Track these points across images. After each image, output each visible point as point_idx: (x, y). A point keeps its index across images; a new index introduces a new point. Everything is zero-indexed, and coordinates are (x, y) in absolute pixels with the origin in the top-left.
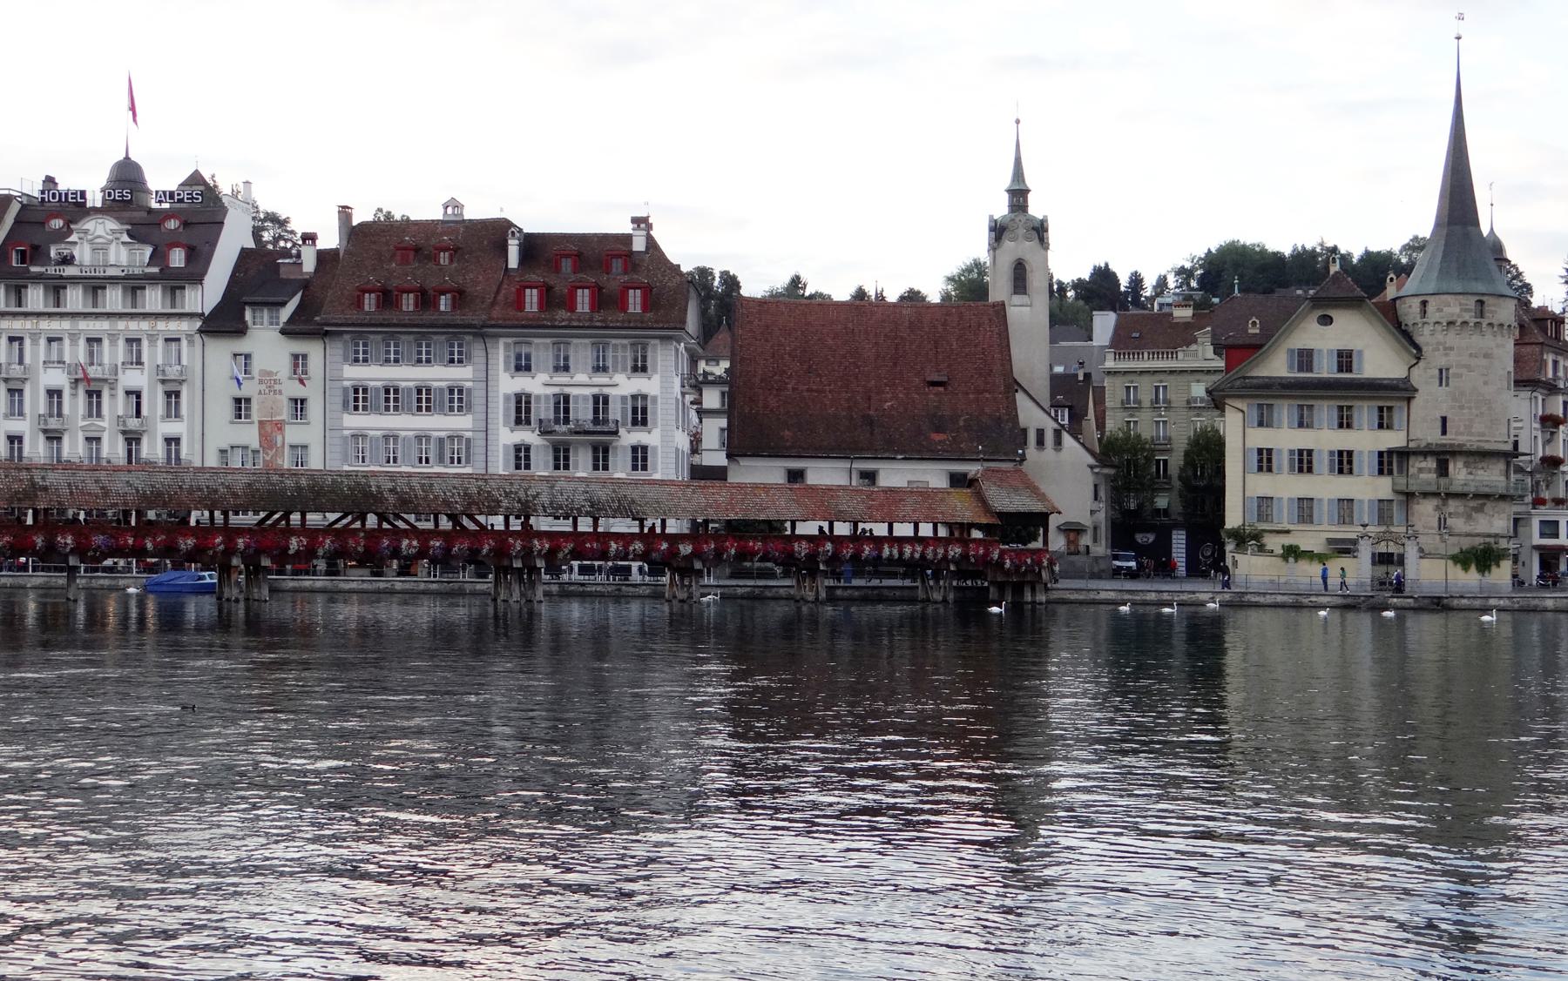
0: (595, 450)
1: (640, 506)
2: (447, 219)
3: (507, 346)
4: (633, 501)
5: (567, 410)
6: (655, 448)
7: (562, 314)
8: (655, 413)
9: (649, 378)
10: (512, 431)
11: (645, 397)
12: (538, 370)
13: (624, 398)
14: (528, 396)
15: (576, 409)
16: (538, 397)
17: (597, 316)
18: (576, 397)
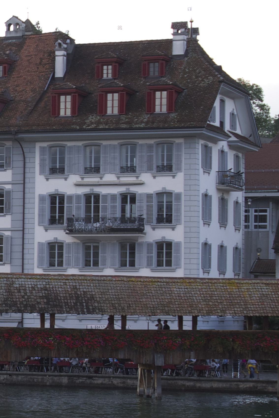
0: (123, 247)
1: (99, 302)
2: (9, 36)
3: (42, 150)
4: (92, 297)
5: (97, 209)
6: (178, 244)
7: (92, 118)
8: (178, 210)
9: (174, 177)
10: (46, 230)
11: (169, 194)
12: (71, 172)
13: (149, 196)
14: (62, 198)
15: (105, 208)
16: (70, 198)
17: (123, 117)
18: (105, 196)
